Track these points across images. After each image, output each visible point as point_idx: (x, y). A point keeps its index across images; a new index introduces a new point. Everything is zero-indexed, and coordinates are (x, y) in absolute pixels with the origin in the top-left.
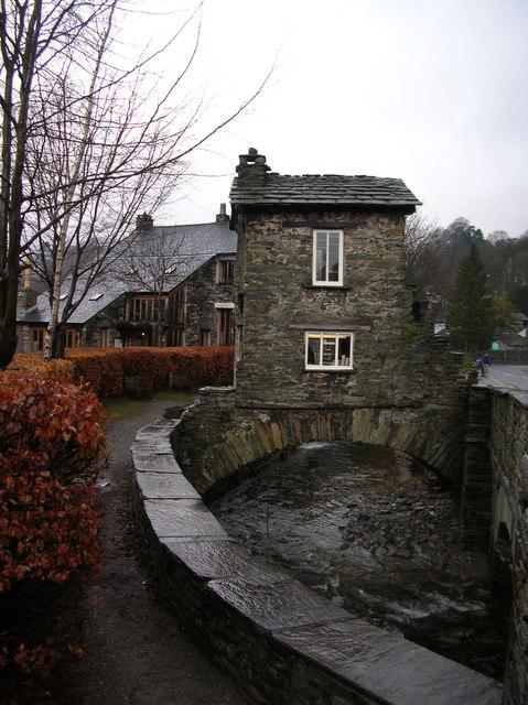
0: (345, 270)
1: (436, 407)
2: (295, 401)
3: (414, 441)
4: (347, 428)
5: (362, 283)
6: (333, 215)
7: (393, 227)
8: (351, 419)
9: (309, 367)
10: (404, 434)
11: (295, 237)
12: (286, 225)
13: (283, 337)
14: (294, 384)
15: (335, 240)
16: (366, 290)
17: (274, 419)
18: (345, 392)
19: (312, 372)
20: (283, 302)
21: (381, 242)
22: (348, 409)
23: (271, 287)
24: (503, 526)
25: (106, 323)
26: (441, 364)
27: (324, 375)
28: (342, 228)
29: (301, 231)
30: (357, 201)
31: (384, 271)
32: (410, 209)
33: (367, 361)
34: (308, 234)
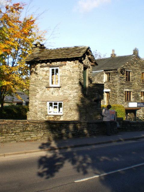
5: (65, 85)
6: (55, 63)
11: (43, 71)
16: (66, 87)
20: (40, 92)
27: (53, 116)
31: (72, 80)
34: (48, 69)
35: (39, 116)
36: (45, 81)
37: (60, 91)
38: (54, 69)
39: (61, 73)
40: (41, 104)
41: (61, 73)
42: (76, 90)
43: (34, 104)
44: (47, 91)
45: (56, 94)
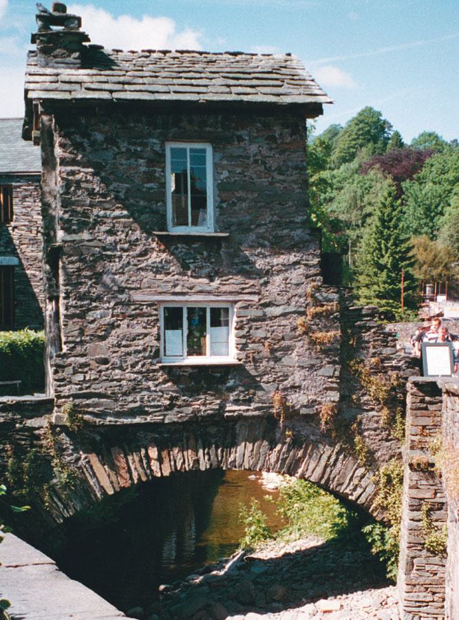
15: (199, 158)
21: (270, 162)
38: (185, 150)
39: (227, 174)
41: (227, 174)
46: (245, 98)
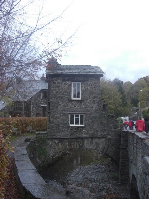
0: (82, 95)
1: (111, 137)
2: (67, 136)
3: (104, 148)
4: (83, 144)
7: (96, 81)
8: (84, 142)
9: (71, 125)
10: (101, 146)
11: (66, 84)
12: (63, 80)
13: (63, 116)
14: (65, 131)
17: (59, 142)
18: (82, 133)
19: (72, 127)
21: (93, 86)
22: (83, 139)
23: (59, 100)
24: (133, 176)
25: (6, 111)
26: (112, 124)
28: (80, 82)
29: (68, 82)
30: (85, 73)
31: (94, 95)
32: (102, 76)
33: (89, 123)
34: (70, 83)
35: (60, 127)
36: (67, 94)
37: (82, 104)
40: (63, 116)
42: (97, 104)
43: (55, 116)
44: (70, 104)
45: (78, 106)
46: (88, 73)
